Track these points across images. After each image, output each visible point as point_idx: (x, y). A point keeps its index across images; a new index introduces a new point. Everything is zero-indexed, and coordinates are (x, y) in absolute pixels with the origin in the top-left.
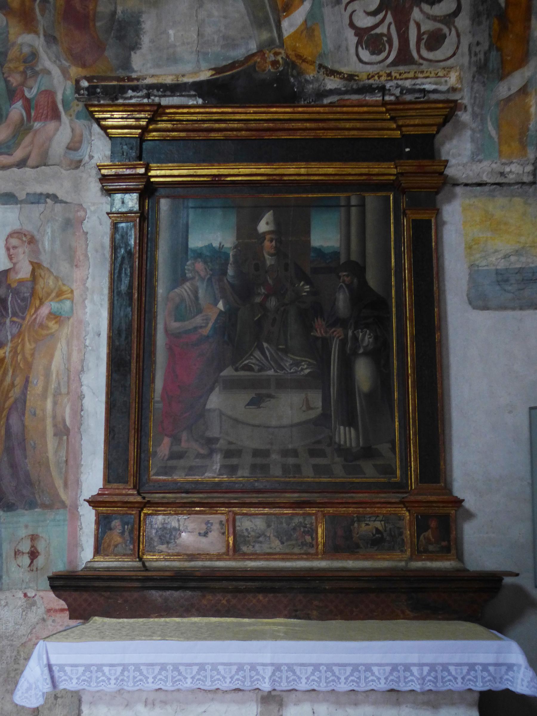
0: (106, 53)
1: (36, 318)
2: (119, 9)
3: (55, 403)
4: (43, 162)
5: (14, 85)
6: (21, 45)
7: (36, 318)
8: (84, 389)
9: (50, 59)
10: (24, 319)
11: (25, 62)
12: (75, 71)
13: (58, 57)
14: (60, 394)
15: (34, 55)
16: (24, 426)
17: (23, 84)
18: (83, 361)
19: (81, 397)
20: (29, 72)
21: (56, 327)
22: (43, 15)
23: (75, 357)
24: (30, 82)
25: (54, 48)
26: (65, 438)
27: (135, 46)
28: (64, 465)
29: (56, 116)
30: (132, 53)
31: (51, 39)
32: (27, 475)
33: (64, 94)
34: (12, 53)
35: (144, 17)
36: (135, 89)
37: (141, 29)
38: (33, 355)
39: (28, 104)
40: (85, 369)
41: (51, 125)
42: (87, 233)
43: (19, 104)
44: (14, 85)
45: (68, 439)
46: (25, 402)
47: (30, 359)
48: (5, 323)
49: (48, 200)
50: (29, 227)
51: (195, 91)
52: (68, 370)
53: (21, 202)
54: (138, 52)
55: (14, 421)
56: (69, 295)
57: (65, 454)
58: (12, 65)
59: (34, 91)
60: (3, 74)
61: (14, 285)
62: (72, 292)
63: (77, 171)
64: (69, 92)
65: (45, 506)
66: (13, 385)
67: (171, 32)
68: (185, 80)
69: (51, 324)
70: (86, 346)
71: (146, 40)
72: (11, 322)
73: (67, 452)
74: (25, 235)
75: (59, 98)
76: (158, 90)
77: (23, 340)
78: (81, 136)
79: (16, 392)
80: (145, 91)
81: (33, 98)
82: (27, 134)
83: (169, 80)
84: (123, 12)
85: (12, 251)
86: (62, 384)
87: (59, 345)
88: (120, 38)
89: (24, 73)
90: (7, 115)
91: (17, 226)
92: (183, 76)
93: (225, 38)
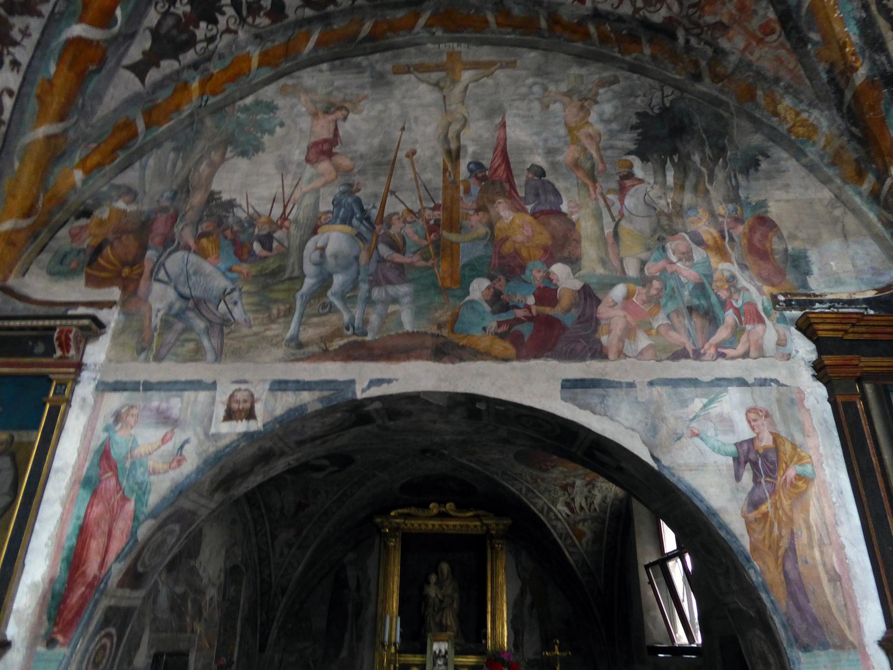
0: (788, 277)
1: (786, 479)
2: (790, 248)
3: (822, 552)
4: (762, 354)
5: (724, 298)
6: (722, 270)
7: (786, 479)
8: (843, 539)
9: (746, 280)
10: (776, 479)
11: (728, 281)
12: (767, 289)
13: (751, 279)
14: (824, 544)
15: (733, 277)
16: (799, 573)
17: (730, 297)
18: (835, 515)
19: (842, 547)
20: (733, 289)
21: (805, 486)
22: (732, 248)
23: (828, 512)
24: (735, 296)
25: (747, 273)
26: (838, 583)
27: (808, 273)
28: (843, 608)
29: (761, 321)
30: (807, 277)
31: (743, 267)
32: (815, 619)
33: (763, 304)
34: (716, 276)
35: (809, 253)
36: (821, 302)
37: (810, 261)
38: (791, 510)
39: (737, 311)
40: (839, 523)
41: (759, 328)
42: (809, 410)
43: (730, 312)
44: (724, 298)
45: (841, 584)
46: (795, 551)
47: (790, 514)
48: (760, 483)
49: (772, 383)
50: (761, 404)
51: (867, 304)
52: (825, 523)
53: (753, 385)
54: (812, 276)
55: (789, 566)
56: (809, 460)
57: (842, 599)
58: (718, 284)
59: (740, 302)
60: (713, 290)
61: (761, 451)
62: (810, 457)
63: (788, 362)
64: (766, 304)
65: (836, 647)
66: (780, 536)
67: (832, 263)
68: (857, 297)
69: (800, 483)
70: (834, 503)
71: (815, 269)
72: (765, 481)
73: (844, 596)
74: (761, 411)
75: (760, 308)
76: (839, 304)
77: (780, 497)
78: (785, 335)
79: (784, 543)
80: (828, 305)
81: (741, 307)
82: (742, 334)
83: (845, 297)
84: (792, 249)
85: (752, 423)
86: (823, 536)
87: (811, 502)
88: (796, 267)
89: (729, 289)
90: (724, 320)
91: (751, 404)
92: (854, 294)
93: (873, 268)
